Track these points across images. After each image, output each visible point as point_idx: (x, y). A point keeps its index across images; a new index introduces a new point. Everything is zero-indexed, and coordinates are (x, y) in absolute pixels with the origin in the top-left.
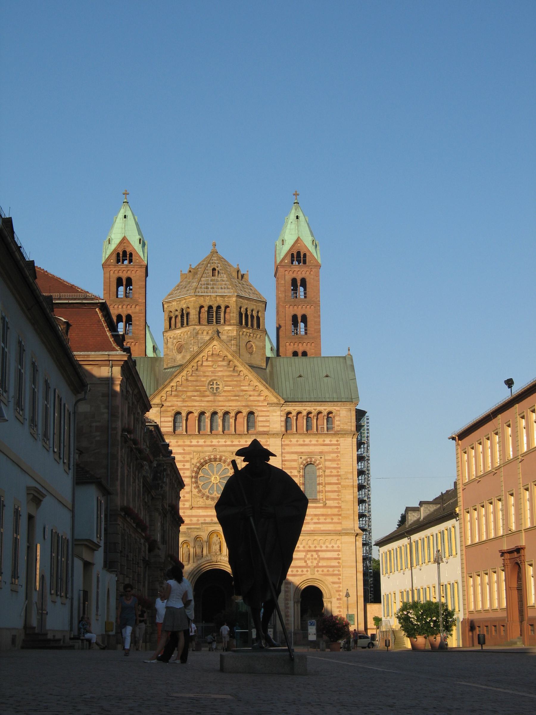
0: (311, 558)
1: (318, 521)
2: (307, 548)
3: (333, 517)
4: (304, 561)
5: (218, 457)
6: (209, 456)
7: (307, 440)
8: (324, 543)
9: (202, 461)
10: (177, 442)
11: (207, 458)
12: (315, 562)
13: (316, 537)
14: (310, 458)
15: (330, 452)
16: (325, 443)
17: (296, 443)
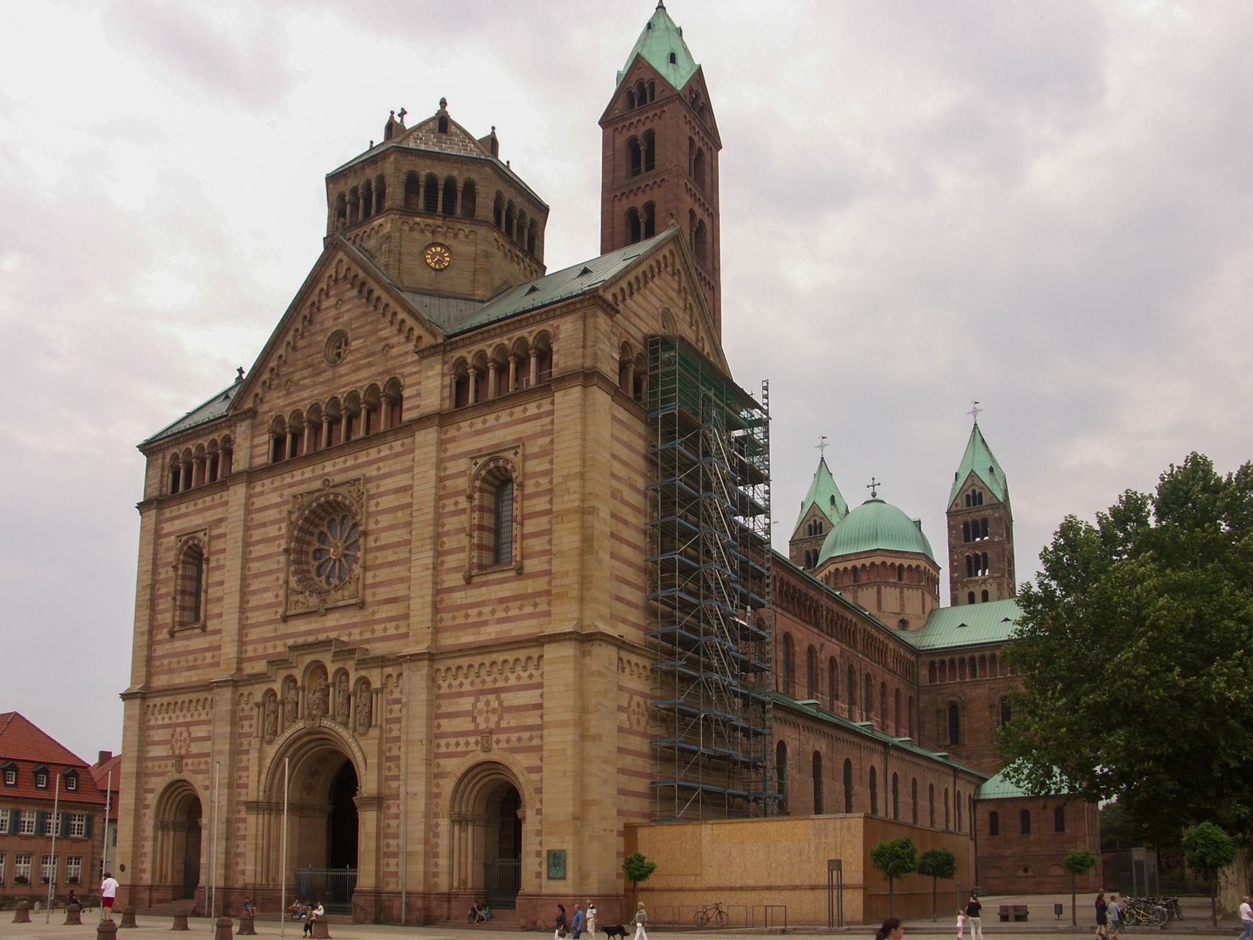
0: (485, 709)
1: (503, 615)
2: (478, 686)
3: (537, 600)
4: (470, 719)
5: (332, 497)
6: (318, 499)
7: (491, 419)
8: (513, 671)
9: (307, 512)
10: (273, 482)
11: (314, 505)
12: (494, 718)
13: (494, 657)
14: (497, 459)
15: (535, 436)
16: (528, 414)
17: (468, 429)
